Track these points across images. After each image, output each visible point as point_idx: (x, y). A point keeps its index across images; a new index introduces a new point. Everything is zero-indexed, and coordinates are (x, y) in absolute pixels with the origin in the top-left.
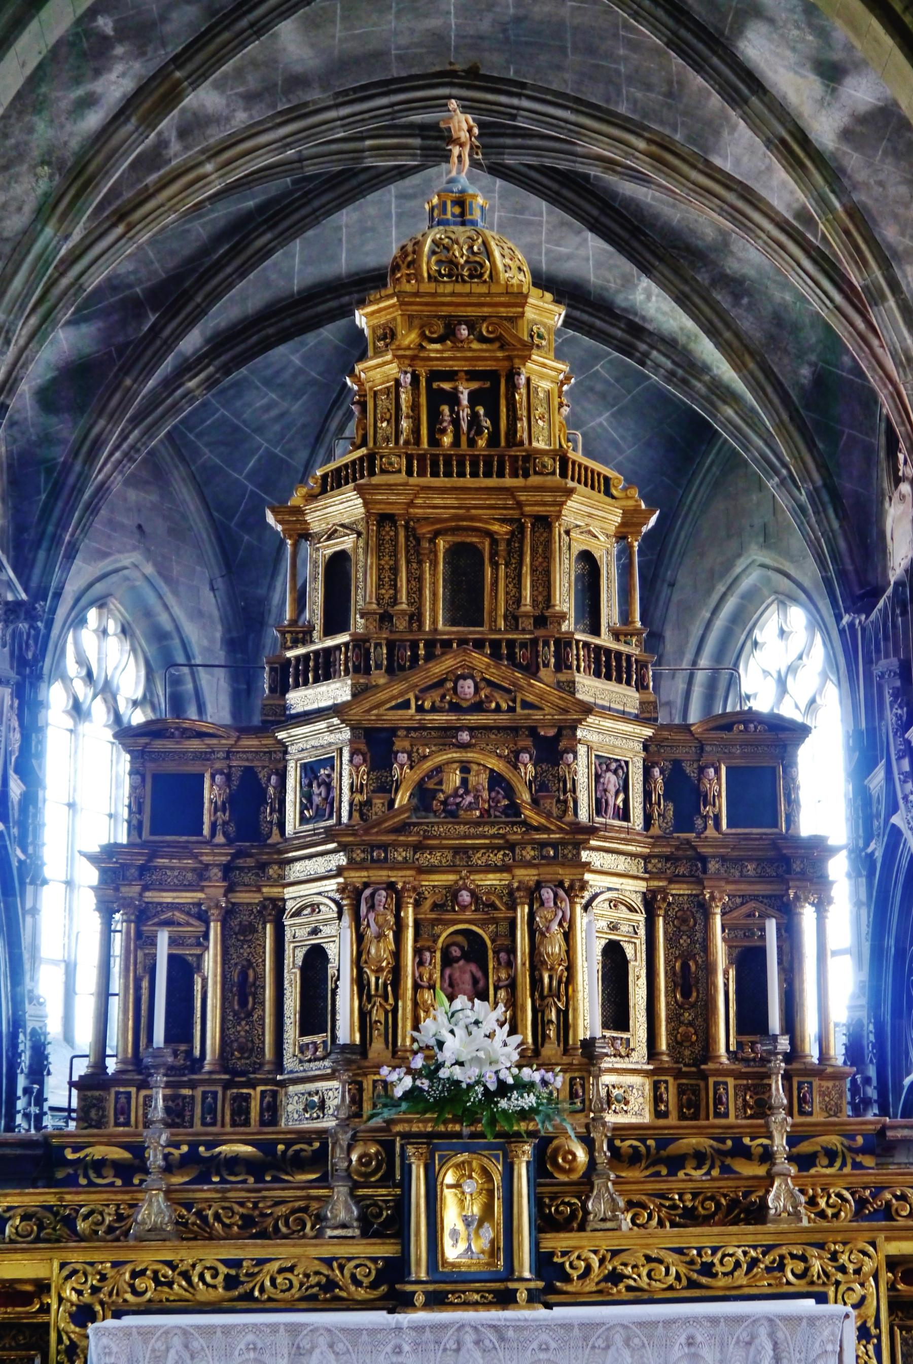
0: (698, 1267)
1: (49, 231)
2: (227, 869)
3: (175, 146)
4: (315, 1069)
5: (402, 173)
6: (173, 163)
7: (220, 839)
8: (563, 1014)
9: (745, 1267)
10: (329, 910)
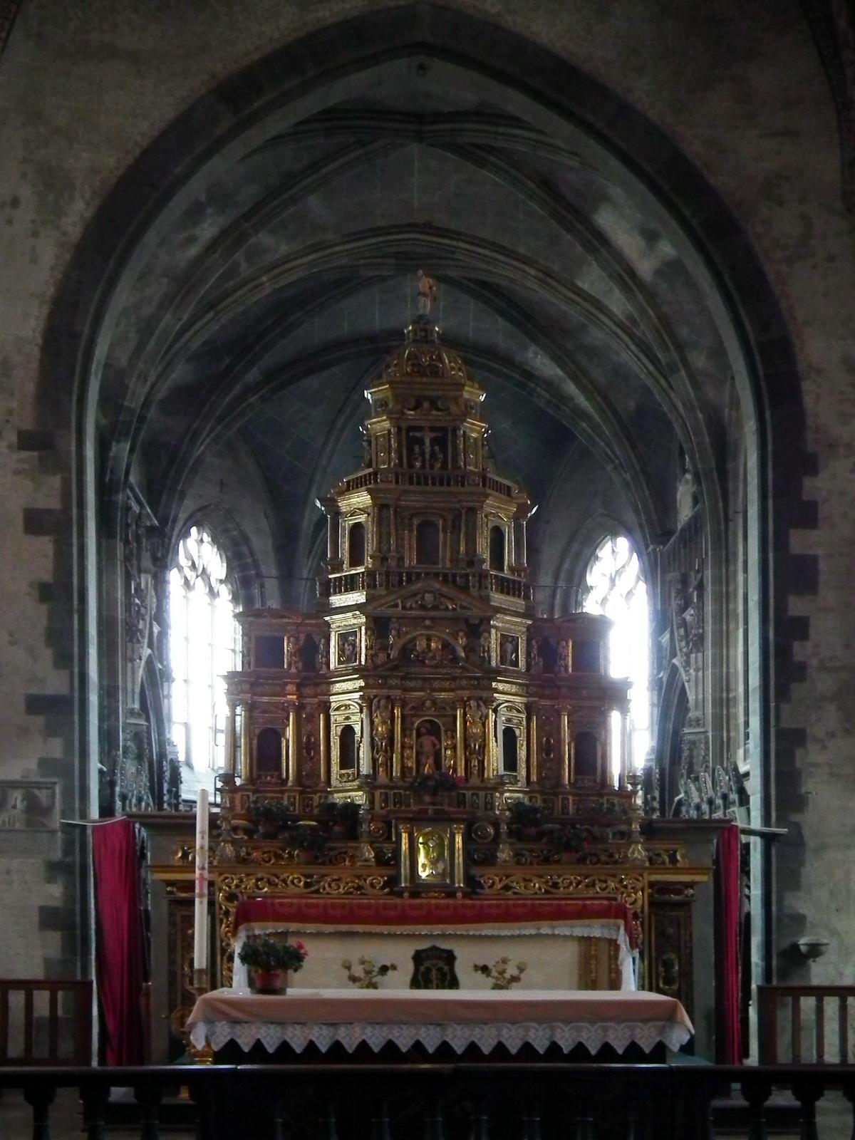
0: (550, 884)
1: (168, 316)
2: (299, 686)
3: (243, 265)
4: (349, 785)
5: (383, 279)
6: (242, 276)
7: (293, 670)
8: (481, 763)
9: (574, 884)
10: (355, 709)
